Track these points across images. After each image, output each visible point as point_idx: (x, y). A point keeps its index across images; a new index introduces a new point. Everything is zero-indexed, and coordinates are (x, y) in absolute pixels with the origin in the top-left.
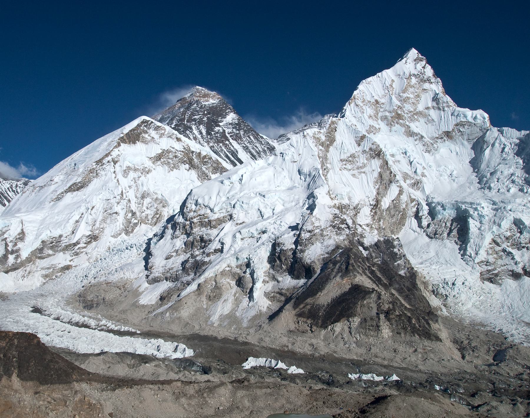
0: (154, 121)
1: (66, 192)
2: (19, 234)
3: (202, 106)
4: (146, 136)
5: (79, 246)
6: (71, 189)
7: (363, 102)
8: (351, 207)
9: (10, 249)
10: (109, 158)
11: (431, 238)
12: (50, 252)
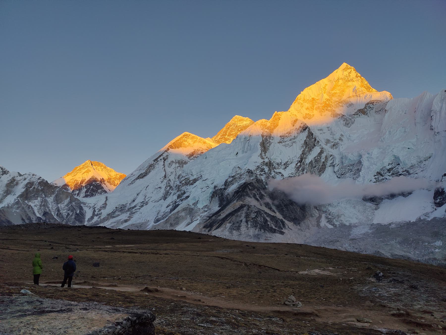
0: (191, 134)
1: (137, 179)
2: (103, 205)
3: (237, 126)
4: (186, 143)
5: (135, 208)
6: (139, 178)
7: (304, 100)
8: (283, 164)
9: (96, 213)
10: (162, 157)
11: (339, 178)
12: (119, 213)
